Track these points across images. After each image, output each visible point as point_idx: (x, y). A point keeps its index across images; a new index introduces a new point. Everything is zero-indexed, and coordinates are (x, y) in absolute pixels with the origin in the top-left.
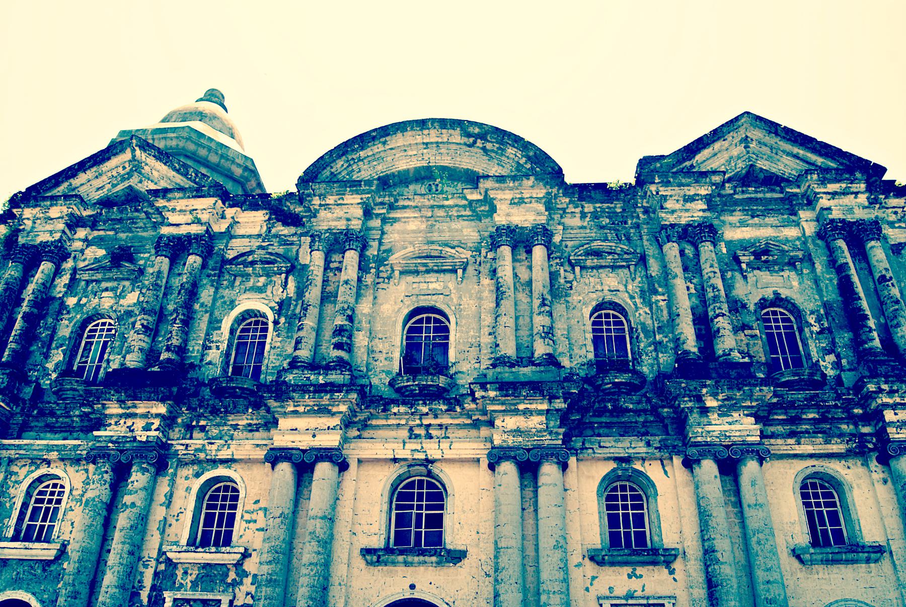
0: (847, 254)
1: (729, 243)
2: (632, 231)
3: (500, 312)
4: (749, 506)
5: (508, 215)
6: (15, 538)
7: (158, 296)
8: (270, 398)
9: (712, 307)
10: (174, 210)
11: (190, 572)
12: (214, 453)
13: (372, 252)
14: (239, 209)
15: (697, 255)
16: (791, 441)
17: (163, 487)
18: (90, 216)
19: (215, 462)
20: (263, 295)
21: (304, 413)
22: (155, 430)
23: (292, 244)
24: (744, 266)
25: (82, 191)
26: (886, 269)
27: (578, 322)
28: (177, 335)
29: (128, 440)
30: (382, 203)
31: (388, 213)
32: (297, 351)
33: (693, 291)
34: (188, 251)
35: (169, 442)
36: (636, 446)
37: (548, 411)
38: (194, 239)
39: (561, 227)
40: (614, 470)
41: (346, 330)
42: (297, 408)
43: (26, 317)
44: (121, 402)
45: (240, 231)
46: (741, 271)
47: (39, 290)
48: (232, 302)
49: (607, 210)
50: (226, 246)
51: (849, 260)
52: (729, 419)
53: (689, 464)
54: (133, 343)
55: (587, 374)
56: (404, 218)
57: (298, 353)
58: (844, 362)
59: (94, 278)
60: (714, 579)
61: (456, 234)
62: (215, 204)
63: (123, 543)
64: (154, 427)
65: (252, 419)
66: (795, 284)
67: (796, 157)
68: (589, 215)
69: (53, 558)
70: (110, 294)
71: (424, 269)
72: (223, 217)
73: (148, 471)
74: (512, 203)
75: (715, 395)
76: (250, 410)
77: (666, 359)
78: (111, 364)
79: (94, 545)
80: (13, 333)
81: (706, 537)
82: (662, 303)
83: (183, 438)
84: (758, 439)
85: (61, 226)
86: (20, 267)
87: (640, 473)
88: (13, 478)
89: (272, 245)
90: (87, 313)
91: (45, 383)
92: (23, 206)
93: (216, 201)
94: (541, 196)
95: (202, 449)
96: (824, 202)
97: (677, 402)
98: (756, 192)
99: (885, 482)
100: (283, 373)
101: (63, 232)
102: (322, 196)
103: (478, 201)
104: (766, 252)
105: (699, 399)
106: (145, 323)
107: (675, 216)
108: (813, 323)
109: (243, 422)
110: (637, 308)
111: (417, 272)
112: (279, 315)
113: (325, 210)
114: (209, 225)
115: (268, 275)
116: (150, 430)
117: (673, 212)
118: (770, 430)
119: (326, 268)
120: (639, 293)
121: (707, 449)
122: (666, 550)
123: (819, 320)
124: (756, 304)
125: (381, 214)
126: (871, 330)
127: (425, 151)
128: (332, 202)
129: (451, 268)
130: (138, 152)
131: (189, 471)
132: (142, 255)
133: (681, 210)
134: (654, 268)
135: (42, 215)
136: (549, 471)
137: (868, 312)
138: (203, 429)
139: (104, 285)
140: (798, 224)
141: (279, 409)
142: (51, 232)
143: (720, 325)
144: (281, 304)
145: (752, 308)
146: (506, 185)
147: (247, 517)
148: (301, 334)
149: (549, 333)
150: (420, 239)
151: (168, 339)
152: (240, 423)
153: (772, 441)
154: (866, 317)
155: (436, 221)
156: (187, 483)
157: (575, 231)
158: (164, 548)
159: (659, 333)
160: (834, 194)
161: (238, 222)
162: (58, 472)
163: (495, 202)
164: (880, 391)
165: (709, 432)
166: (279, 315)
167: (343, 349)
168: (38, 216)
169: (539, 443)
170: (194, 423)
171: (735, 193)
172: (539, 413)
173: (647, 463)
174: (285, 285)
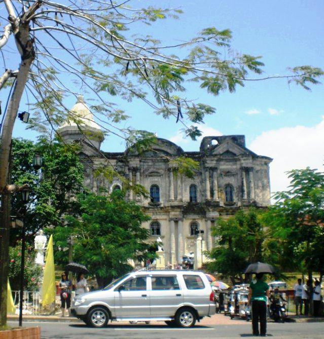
1: (221, 169)
13: (142, 171)
15: (213, 174)
36: (196, 217)
53: (206, 221)
66: (233, 180)
96: (242, 161)
104: (228, 172)
105: (208, 209)
111: (151, 176)
118: (222, 213)
119: (133, 175)
121: (209, 219)
123: (237, 189)
134: (203, 177)
136: (180, 222)
160: (244, 160)
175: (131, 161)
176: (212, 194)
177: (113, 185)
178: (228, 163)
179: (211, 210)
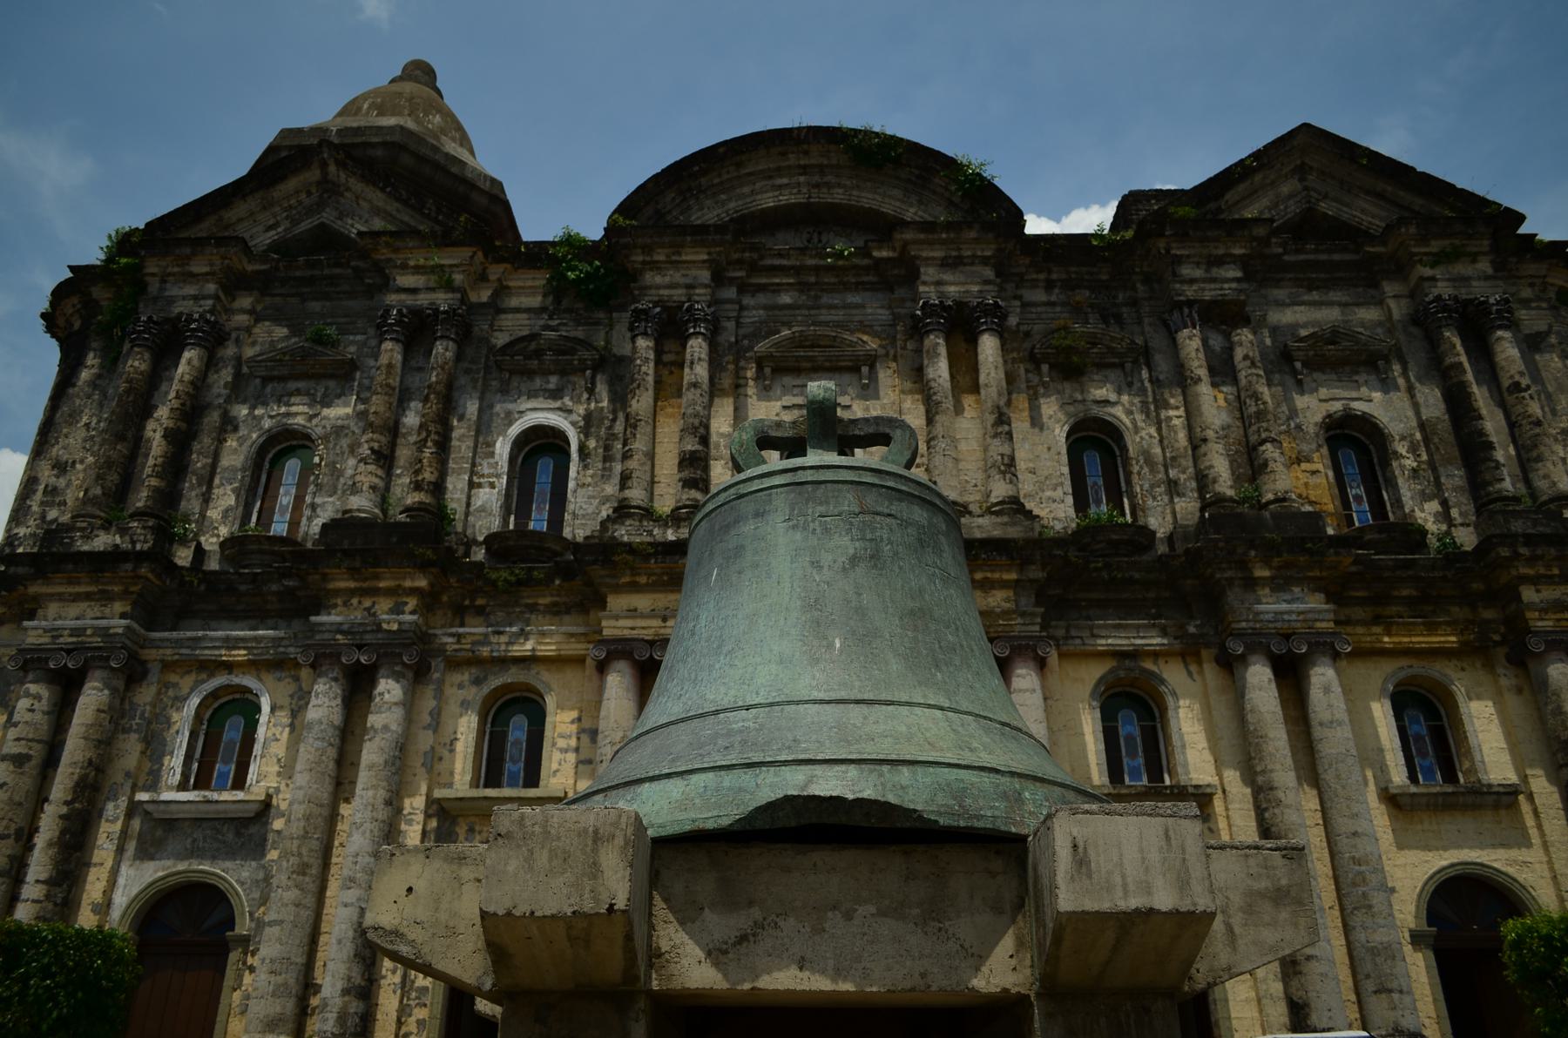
0: (1459, 348)
1: (1274, 330)
2: (1124, 309)
3: (935, 433)
4: (1321, 724)
5: (939, 283)
6: (182, 787)
7: (391, 404)
8: (594, 562)
9: (1254, 428)
10: (404, 267)
11: (477, 828)
12: (503, 647)
13: (728, 335)
14: (509, 266)
16: (1377, 629)
17: (428, 703)
18: (258, 272)
19: (505, 662)
20: (558, 404)
21: (647, 585)
22: (412, 613)
23: (597, 323)
24: (1298, 365)
25: (242, 230)
26: (1521, 374)
27: (1049, 449)
28: (430, 466)
29: (369, 628)
30: (740, 262)
31: (748, 276)
32: (627, 491)
33: (1222, 402)
34: (434, 333)
35: (431, 631)
37: (1017, 581)
38: (445, 312)
39: (1018, 303)
40: (1111, 671)
41: (701, 459)
42: (638, 579)
43: (168, 435)
44: (354, 573)
45: (514, 302)
46: (1294, 372)
47: (187, 393)
48: (509, 414)
49: (1086, 277)
50: (491, 326)
51: (1464, 359)
52: (1287, 596)
54: (358, 478)
55: (1064, 528)
56: (773, 284)
57: (628, 493)
58: (1454, 513)
59: (276, 373)
60: (1273, 829)
61: (854, 312)
62: (472, 257)
63: (374, 787)
64: (408, 608)
65: (558, 595)
67: (1380, 196)
68: (1059, 284)
69: (252, 815)
70: (306, 399)
71: (809, 365)
72: (483, 277)
73: (404, 677)
74: (949, 264)
75: (1267, 563)
76: (557, 582)
77: (1187, 507)
78: (318, 510)
79: (325, 796)
80: (151, 462)
81: (1259, 769)
82: (1176, 422)
83: (452, 626)
84: (1332, 624)
85: (211, 287)
86: (147, 356)
87: (1152, 673)
88: (171, 693)
89: (565, 324)
90: (269, 431)
91: (210, 543)
92: (143, 253)
93: (475, 253)
94: (988, 253)
95: (485, 641)
97: (1209, 571)
98: (1316, 251)
99: (1519, 691)
100: (609, 525)
101: (217, 297)
102: (647, 249)
103: (889, 259)
105: (1243, 565)
106: (376, 446)
107: (1195, 287)
108: (1404, 453)
109: (541, 601)
110: (1137, 430)
112: (587, 436)
113: (651, 270)
114: (464, 292)
115: (563, 373)
116: (403, 613)
117: (1192, 281)
119: (658, 362)
120: (1139, 405)
121: (1258, 643)
122: (1197, 787)
123: (1413, 449)
124: (1316, 424)
125: (737, 278)
126: (1498, 465)
127: (802, 179)
128: (662, 258)
129: (850, 364)
130: (332, 168)
131: (465, 676)
132: (351, 338)
133: (1204, 280)
135: (176, 269)
137: (1494, 439)
138: (481, 611)
139: (292, 385)
140: (1380, 302)
141: (608, 580)
142: (196, 298)
143: (1268, 455)
144: (588, 417)
145: (1312, 430)
146: (936, 236)
147: (562, 743)
148: (632, 464)
149: (1008, 467)
150: (799, 318)
151: (417, 472)
152: (541, 601)
153: (1349, 629)
154: (1490, 446)
155: (822, 290)
156: (462, 694)
157: (1039, 309)
158: (438, 793)
159: (1173, 466)
160: (1437, 260)
161: (508, 287)
162: (249, 681)
163: (918, 262)
164: (1517, 555)
165: (1258, 614)
166: (587, 436)
167: (698, 489)
168: (170, 270)
169: (1007, 629)
170: (467, 602)
171: (1285, 253)
172: (1004, 585)
173: (1161, 662)
174: (591, 391)
175: (655, 266)
176: (1251, 465)
177: (515, 430)
178: (1315, 296)
179: (1261, 572)
